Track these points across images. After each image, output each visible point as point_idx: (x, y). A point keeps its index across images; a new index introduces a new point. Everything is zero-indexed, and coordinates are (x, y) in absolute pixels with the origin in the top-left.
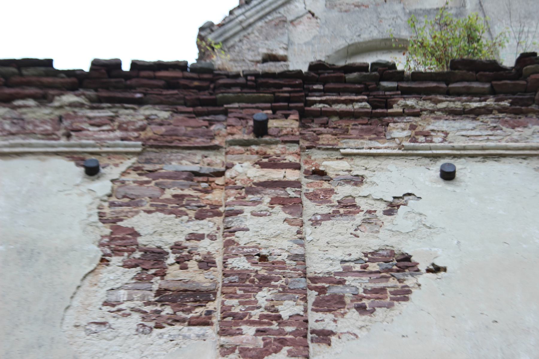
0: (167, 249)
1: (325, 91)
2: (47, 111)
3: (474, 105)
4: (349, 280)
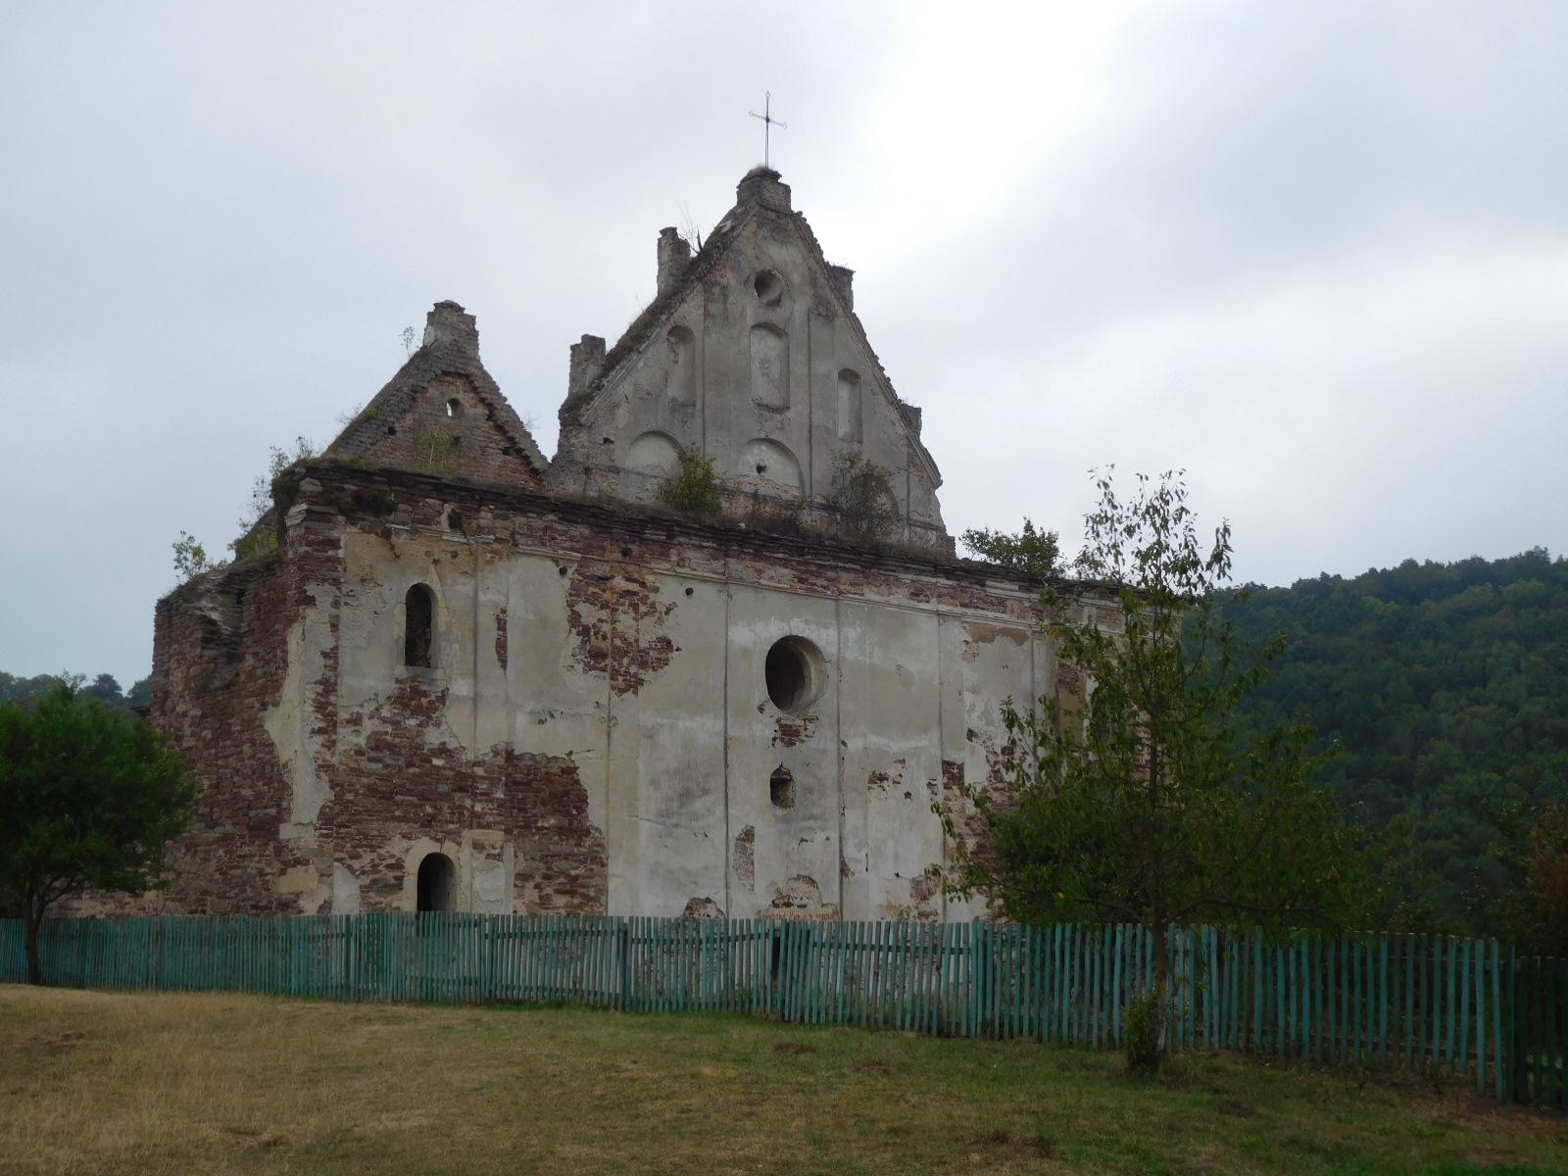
3: (705, 544)
4: (651, 653)
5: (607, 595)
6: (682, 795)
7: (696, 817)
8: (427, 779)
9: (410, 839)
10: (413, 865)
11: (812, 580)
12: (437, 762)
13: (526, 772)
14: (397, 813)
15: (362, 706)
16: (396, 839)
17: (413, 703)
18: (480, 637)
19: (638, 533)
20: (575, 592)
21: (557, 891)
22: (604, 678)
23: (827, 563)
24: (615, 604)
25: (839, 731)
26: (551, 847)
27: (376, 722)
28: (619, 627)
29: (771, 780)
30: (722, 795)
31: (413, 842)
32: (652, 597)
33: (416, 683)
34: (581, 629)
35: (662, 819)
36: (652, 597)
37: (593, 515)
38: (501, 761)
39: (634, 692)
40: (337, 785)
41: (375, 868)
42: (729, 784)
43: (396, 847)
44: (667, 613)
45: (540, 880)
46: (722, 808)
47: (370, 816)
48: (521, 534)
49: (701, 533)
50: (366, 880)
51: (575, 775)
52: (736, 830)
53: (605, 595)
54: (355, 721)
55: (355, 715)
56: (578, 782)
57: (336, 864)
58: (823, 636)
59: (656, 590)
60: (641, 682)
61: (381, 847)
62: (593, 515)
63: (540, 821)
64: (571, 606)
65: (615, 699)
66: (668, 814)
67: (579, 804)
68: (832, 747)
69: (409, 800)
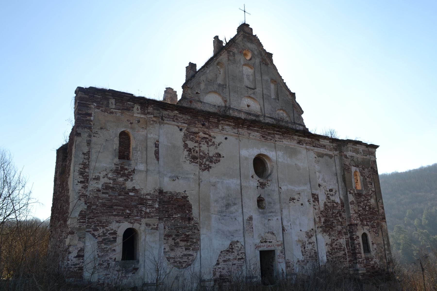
1: (212, 118)
2: (173, 114)
3: (231, 124)
4: (214, 157)
5: (197, 139)
6: (226, 205)
7: (232, 213)
8: (128, 200)
9: (120, 223)
10: (121, 232)
11: (266, 137)
12: (131, 194)
13: (168, 198)
14: (114, 213)
15: (100, 173)
16: (114, 223)
17: (122, 172)
18: (148, 149)
19: (207, 119)
20: (186, 137)
21: (181, 241)
22: (197, 165)
23: (271, 132)
25: (278, 184)
26: (179, 224)
27: (106, 179)
29: (257, 200)
30: (241, 205)
31: (121, 224)
32: (213, 140)
33: (123, 165)
35: (219, 214)
36: (213, 140)
38: (157, 194)
39: (208, 171)
40: (88, 203)
41: (104, 234)
42: (243, 201)
43: (114, 226)
44: (219, 145)
45: (174, 237)
46: (241, 210)
47: (103, 214)
48: (165, 117)
49: (229, 120)
50: (100, 239)
51: (187, 199)
52: (246, 218)
53: (196, 138)
54: (97, 179)
55: (97, 176)
56: (188, 201)
57: (87, 233)
58: (271, 154)
59: (215, 138)
60: (211, 167)
61: (107, 226)
63: (174, 215)
64: (184, 141)
65: (201, 173)
66: (222, 212)
67: (188, 209)
68: (277, 189)
69: (119, 208)
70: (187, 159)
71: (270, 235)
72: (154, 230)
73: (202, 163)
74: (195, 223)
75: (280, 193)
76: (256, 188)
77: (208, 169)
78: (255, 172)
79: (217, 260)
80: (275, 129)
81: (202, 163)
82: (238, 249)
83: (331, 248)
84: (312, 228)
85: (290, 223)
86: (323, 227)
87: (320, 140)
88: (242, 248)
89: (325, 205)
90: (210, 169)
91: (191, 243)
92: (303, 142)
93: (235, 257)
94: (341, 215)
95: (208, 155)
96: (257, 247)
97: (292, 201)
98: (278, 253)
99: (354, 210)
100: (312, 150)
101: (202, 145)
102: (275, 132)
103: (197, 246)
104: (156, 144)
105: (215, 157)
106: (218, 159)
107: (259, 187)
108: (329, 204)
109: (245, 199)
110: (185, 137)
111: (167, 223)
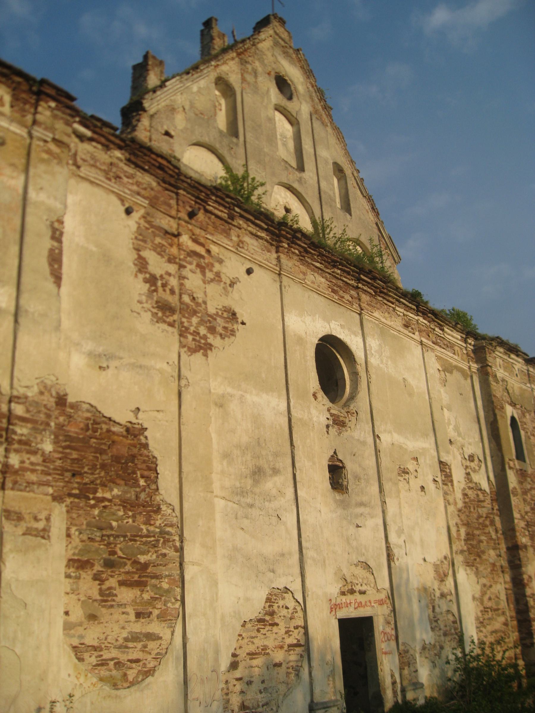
0: (158, 276)
1: (216, 201)
2: (106, 157)
3: (259, 234)
4: (219, 319)
6: (254, 473)
7: (269, 498)
21: (122, 583)
22: (173, 333)
24: (184, 260)
28: (188, 284)
29: (330, 467)
30: (290, 476)
32: (217, 267)
34: (148, 276)
35: (236, 499)
36: (217, 265)
37: (161, 167)
42: (297, 465)
46: (292, 490)
56: (146, 446)
59: (221, 261)
62: (161, 167)
63: (100, 490)
64: (138, 250)
67: (146, 473)
68: (370, 440)
70: (145, 305)
71: (360, 572)
72: (36, 536)
73: (187, 329)
74: (165, 525)
75: (377, 451)
76: (325, 429)
77: (206, 350)
78: (320, 384)
79: (232, 651)
80: (362, 276)
81: (187, 329)
82: (286, 614)
83: (482, 608)
84: (444, 553)
85: (403, 537)
86: (465, 551)
87: (446, 329)
88: (297, 612)
89: (465, 495)
90: (209, 352)
91: (152, 594)
92: (413, 326)
93: (280, 639)
94: (492, 523)
95: (203, 306)
96: (334, 607)
97: (402, 476)
98: (379, 626)
99: (520, 511)
100: (433, 350)
101: (186, 272)
102: (360, 285)
103: (173, 604)
104: (54, 231)
105: (221, 317)
106: (229, 326)
107: (330, 428)
108: (470, 492)
109: (302, 461)
110: (140, 237)
111: (74, 516)
